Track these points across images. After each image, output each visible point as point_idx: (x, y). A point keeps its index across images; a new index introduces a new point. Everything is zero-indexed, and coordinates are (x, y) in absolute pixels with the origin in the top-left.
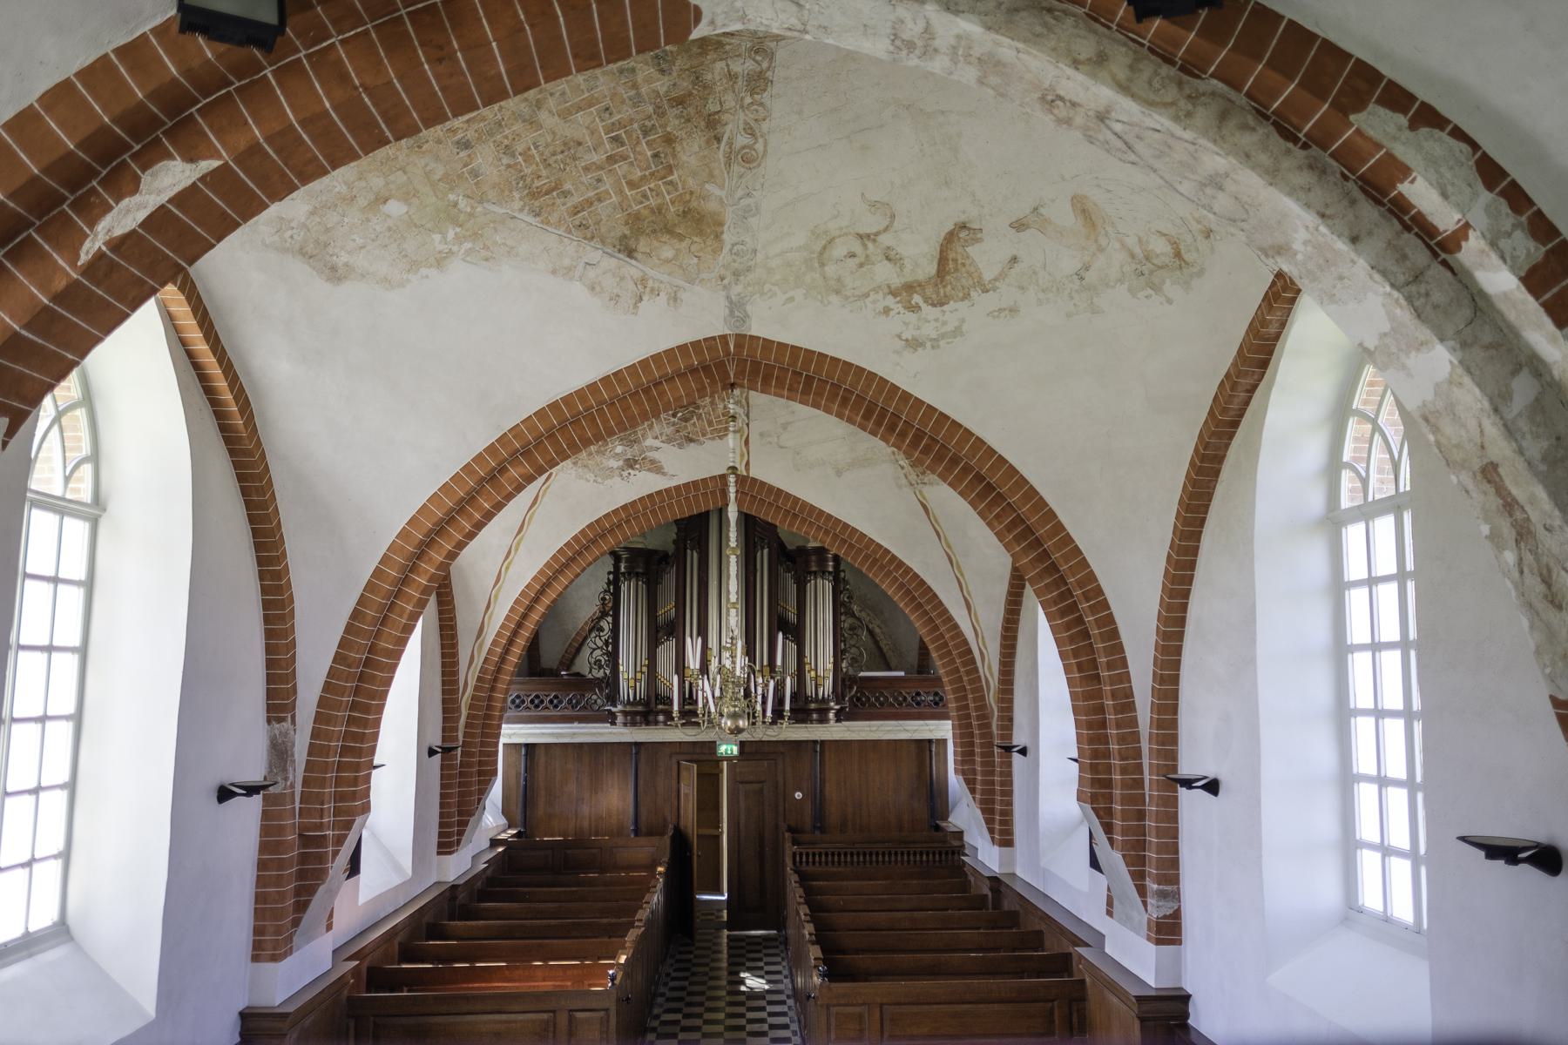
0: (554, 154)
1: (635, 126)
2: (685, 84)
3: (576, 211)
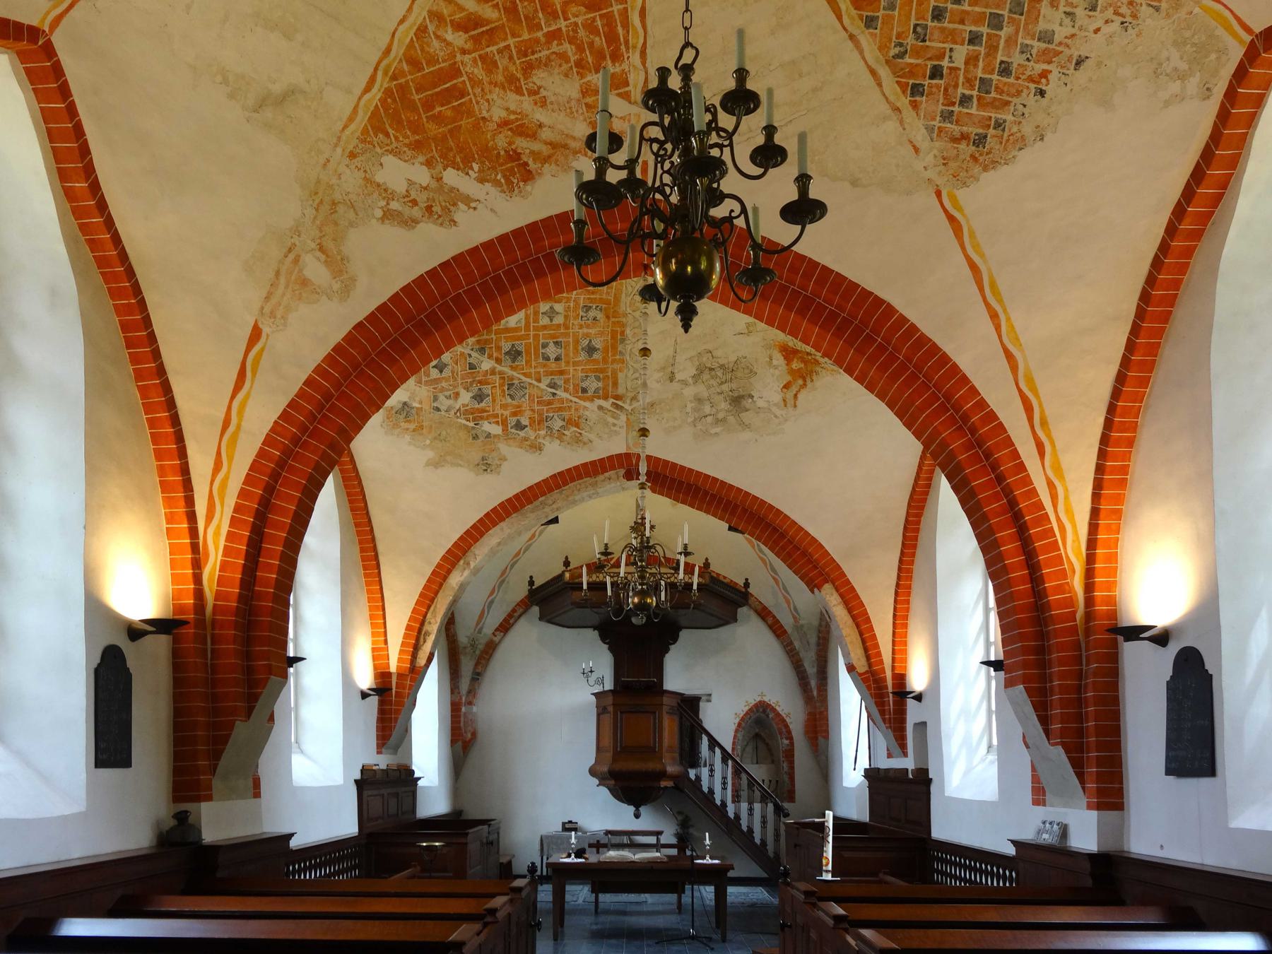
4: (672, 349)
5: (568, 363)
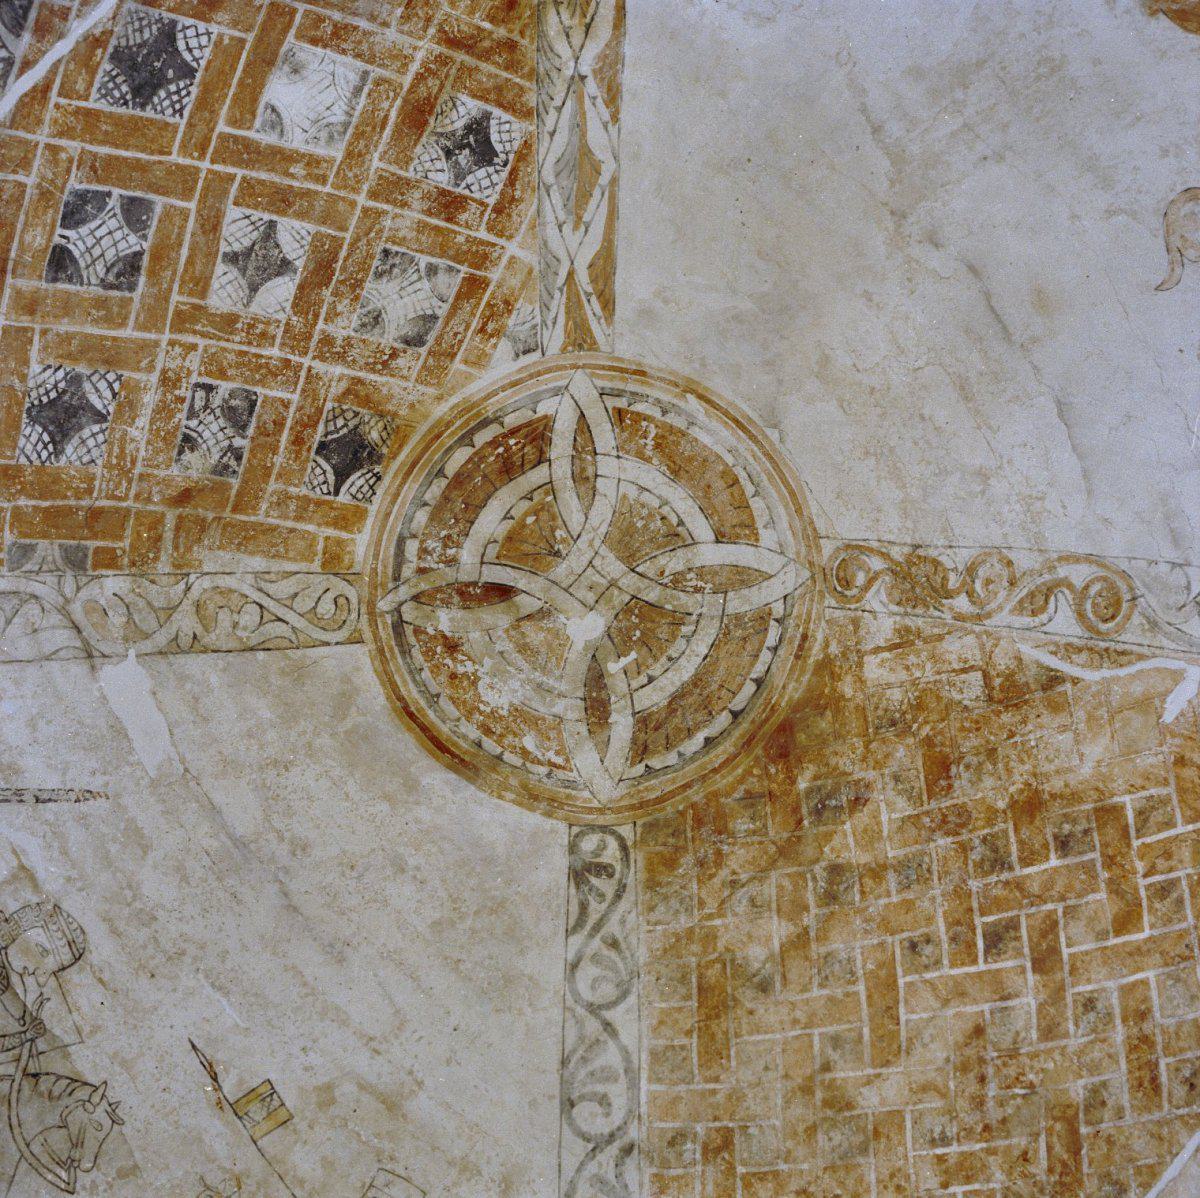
0: (979, 1103)
1: (974, 885)
2: (904, 754)
3: (1148, 1085)
4: (52, 782)
5: (29, 305)
